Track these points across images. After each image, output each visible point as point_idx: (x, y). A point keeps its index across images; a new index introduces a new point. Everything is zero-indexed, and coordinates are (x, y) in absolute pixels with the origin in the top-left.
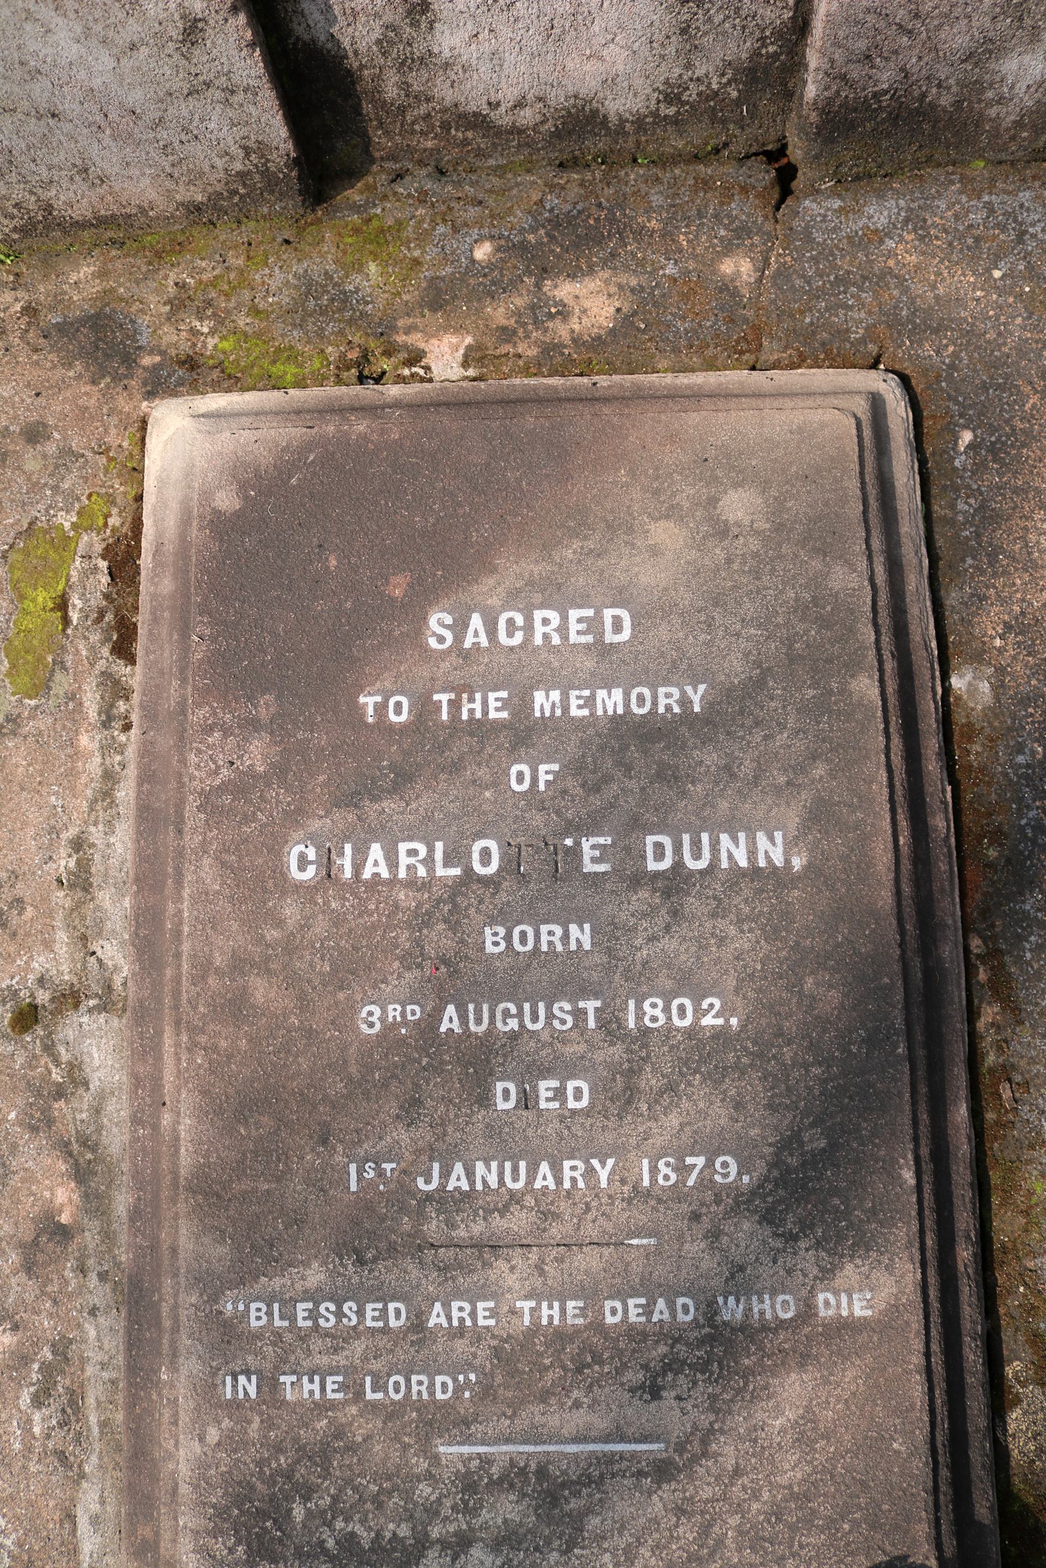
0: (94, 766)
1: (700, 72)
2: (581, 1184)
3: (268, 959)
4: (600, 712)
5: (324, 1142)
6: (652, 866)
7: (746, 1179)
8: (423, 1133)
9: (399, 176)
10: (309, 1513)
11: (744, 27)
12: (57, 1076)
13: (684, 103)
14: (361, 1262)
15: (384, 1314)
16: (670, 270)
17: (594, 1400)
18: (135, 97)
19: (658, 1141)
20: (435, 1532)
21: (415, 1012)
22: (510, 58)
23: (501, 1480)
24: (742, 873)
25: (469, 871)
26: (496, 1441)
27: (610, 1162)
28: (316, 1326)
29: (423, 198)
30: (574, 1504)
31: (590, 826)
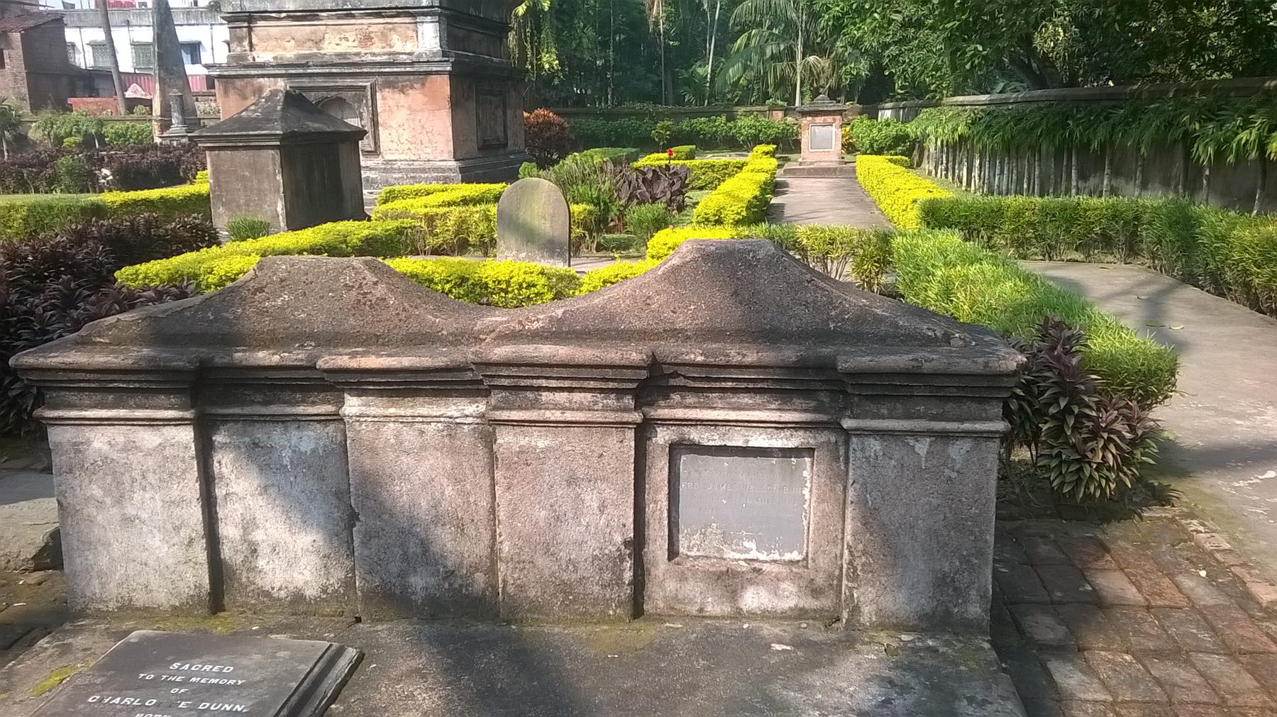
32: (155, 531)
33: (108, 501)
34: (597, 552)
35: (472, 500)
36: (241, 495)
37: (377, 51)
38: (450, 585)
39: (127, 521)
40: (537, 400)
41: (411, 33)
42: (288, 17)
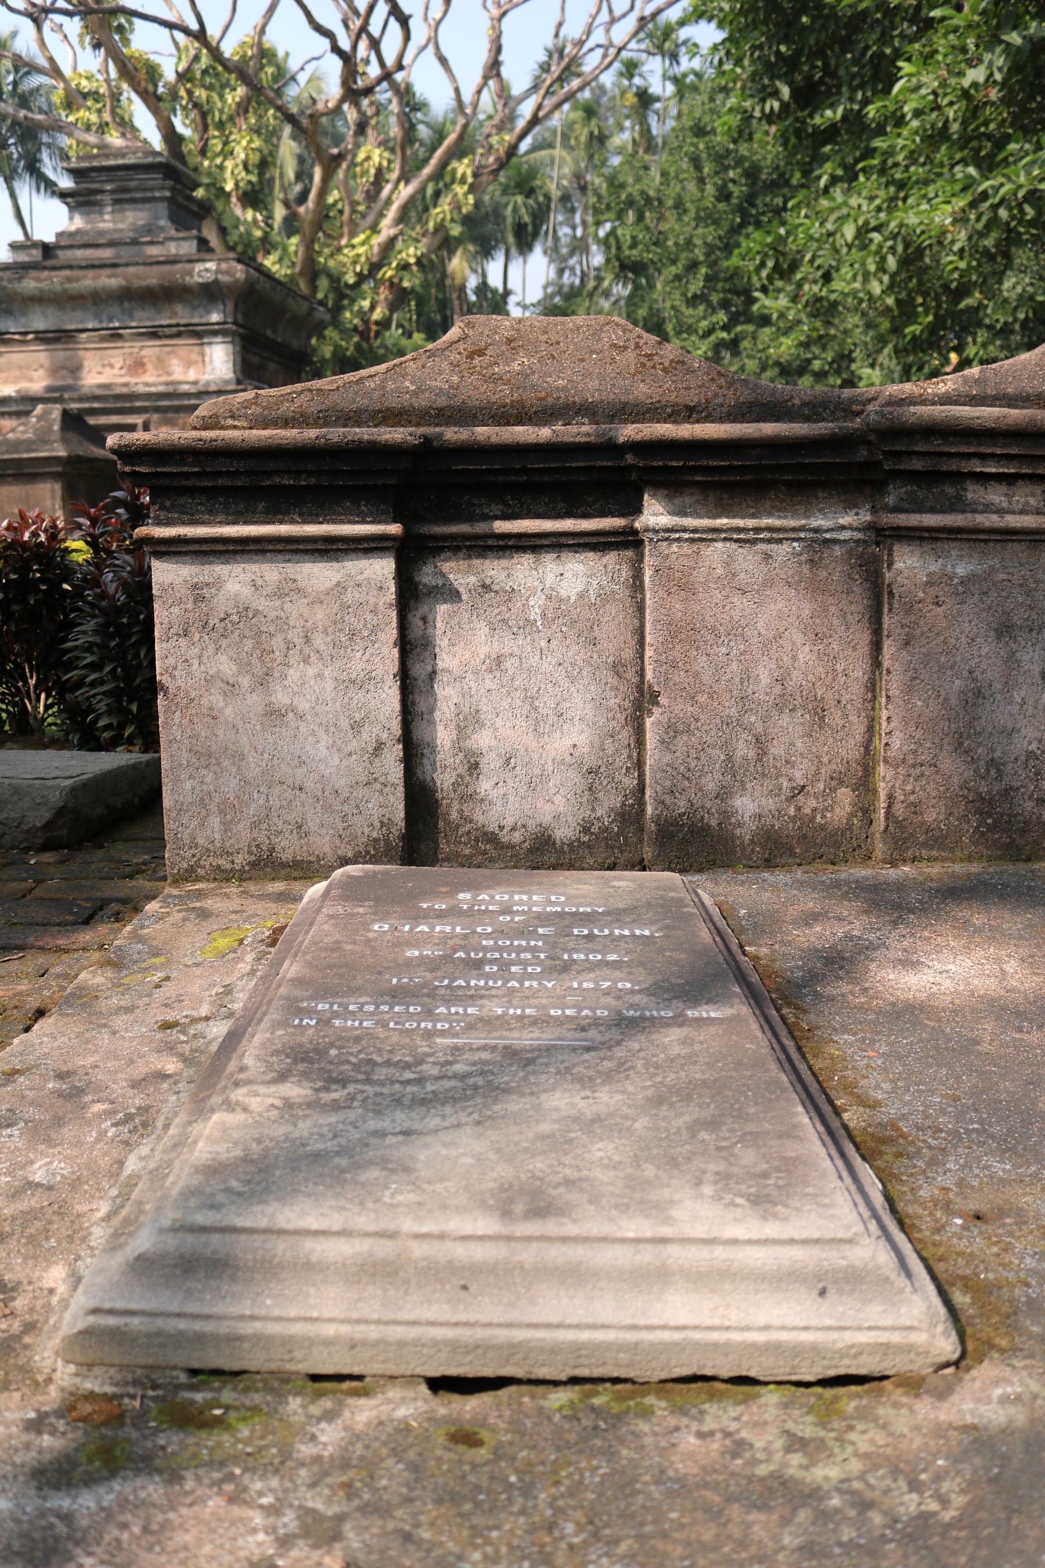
18: (341, 783)
22: (511, 798)
32: (320, 732)
33: (245, 681)
34: (1033, 747)
35: (839, 668)
36: (457, 672)
37: (150, 381)
38: (798, 809)
39: (275, 714)
40: (959, 498)
41: (195, 357)
42: (37, 339)
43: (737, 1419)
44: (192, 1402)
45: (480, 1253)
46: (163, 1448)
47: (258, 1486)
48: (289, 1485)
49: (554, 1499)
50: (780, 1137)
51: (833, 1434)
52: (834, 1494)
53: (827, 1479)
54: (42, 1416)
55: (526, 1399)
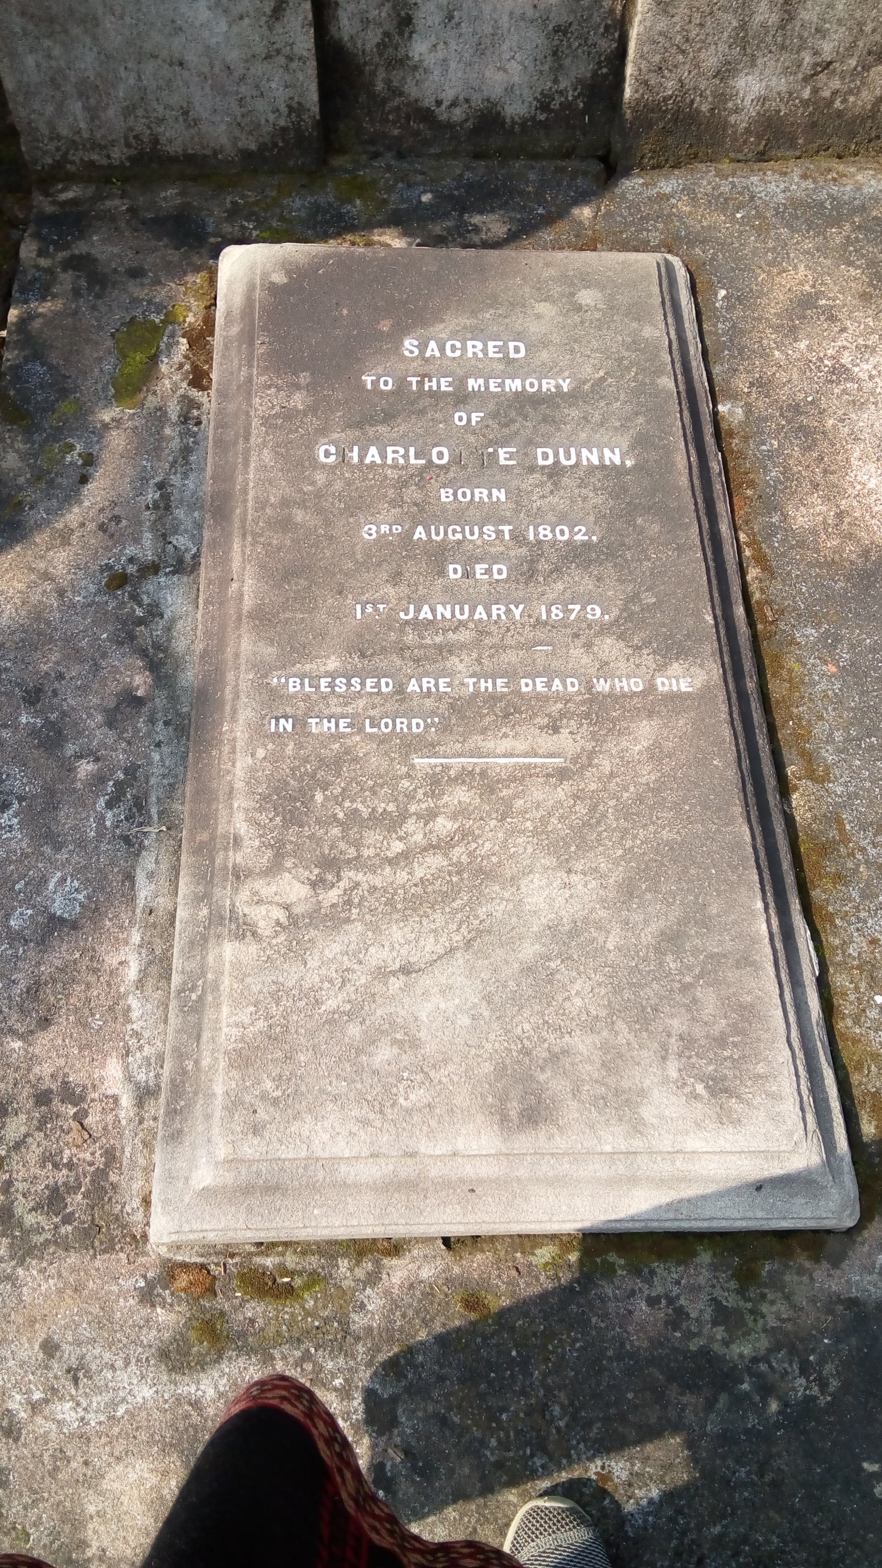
0: (175, 444)
1: (562, 86)
2: (503, 617)
3: (304, 501)
4: (508, 390)
5: (340, 593)
6: (541, 462)
7: (607, 617)
8: (403, 589)
9: (376, 156)
10: (326, 798)
11: (589, 53)
12: (139, 612)
13: (552, 111)
14: (363, 656)
15: (378, 685)
16: (541, 211)
17: (516, 733)
18: (234, 56)
19: (551, 596)
20: (413, 808)
21: (397, 529)
22: (453, 65)
23: (456, 779)
24: (597, 468)
25: (430, 462)
26: (454, 756)
27: (521, 607)
28: (333, 692)
29: (389, 168)
30: (505, 792)
31: (504, 443)
43: (678, 1283)
44: (265, 1268)
45: (487, 1170)
46: (252, 1321)
47: (330, 1365)
48: (352, 1363)
49: (545, 1375)
50: (738, 965)
51: (749, 1305)
52: (747, 1379)
53: (741, 1356)
54: (151, 1285)
55: (518, 1255)
